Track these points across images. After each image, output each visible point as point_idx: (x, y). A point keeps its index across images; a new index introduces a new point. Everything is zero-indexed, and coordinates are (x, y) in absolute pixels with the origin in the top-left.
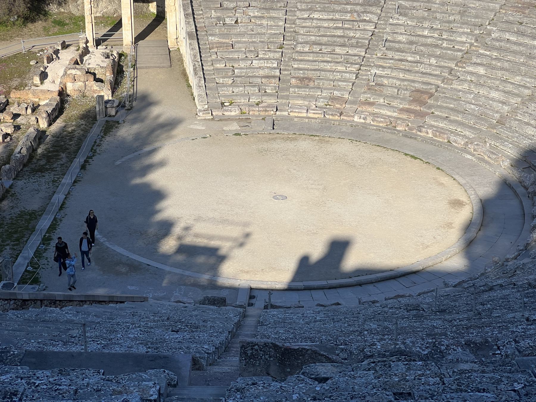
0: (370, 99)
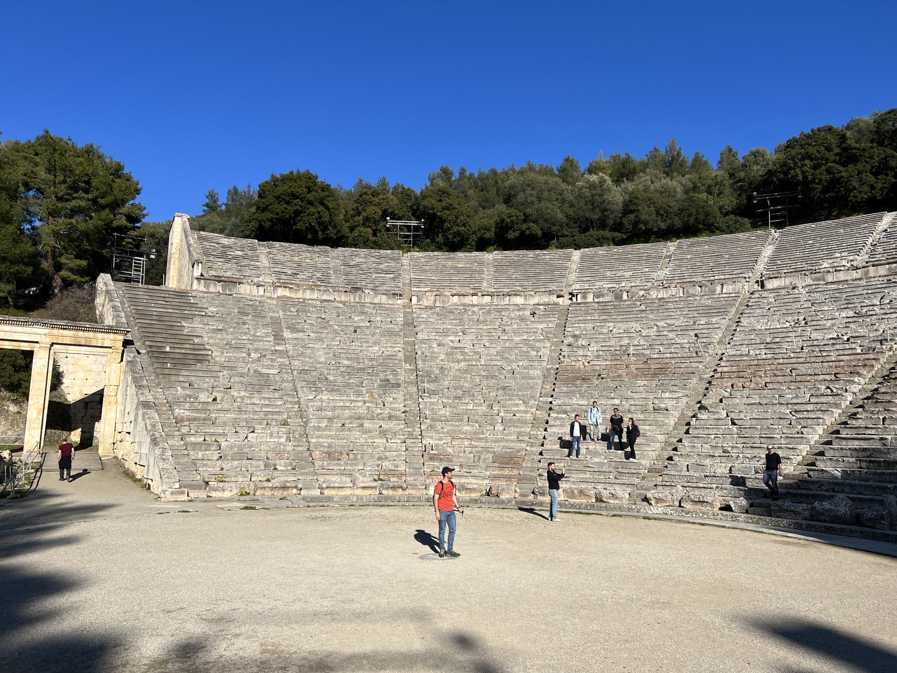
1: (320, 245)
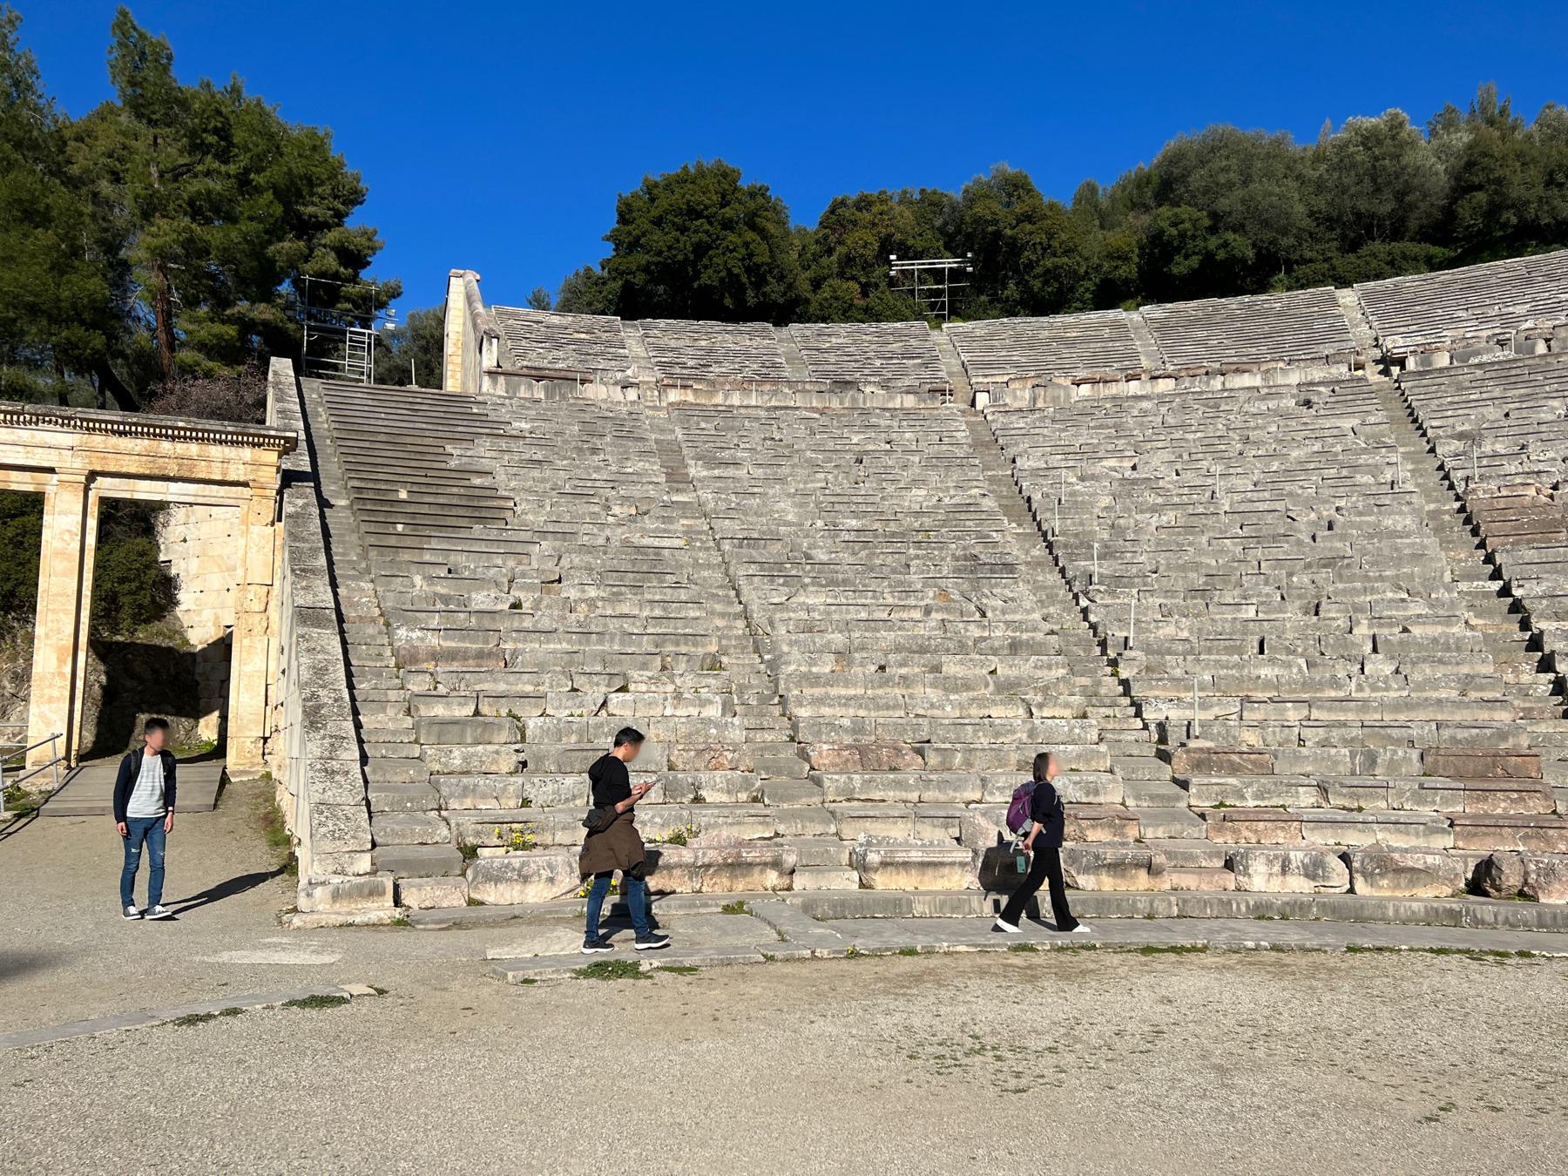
0: (1243, 797)
1: (751, 321)
